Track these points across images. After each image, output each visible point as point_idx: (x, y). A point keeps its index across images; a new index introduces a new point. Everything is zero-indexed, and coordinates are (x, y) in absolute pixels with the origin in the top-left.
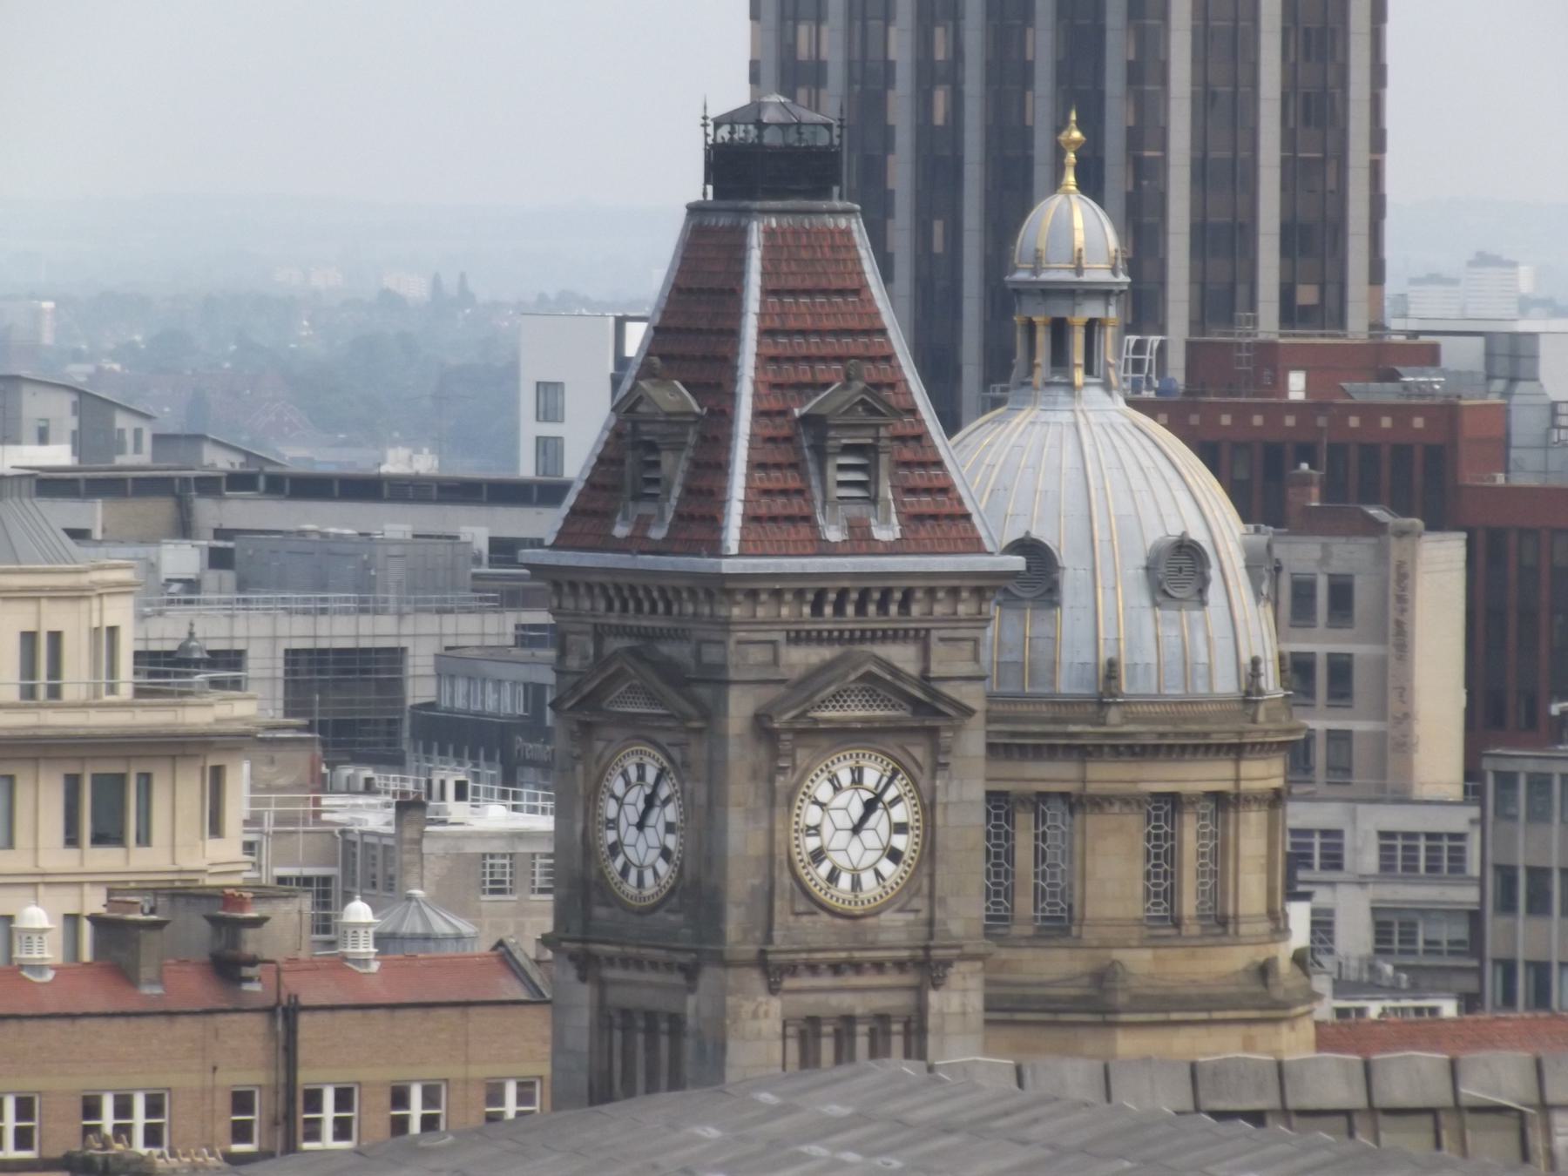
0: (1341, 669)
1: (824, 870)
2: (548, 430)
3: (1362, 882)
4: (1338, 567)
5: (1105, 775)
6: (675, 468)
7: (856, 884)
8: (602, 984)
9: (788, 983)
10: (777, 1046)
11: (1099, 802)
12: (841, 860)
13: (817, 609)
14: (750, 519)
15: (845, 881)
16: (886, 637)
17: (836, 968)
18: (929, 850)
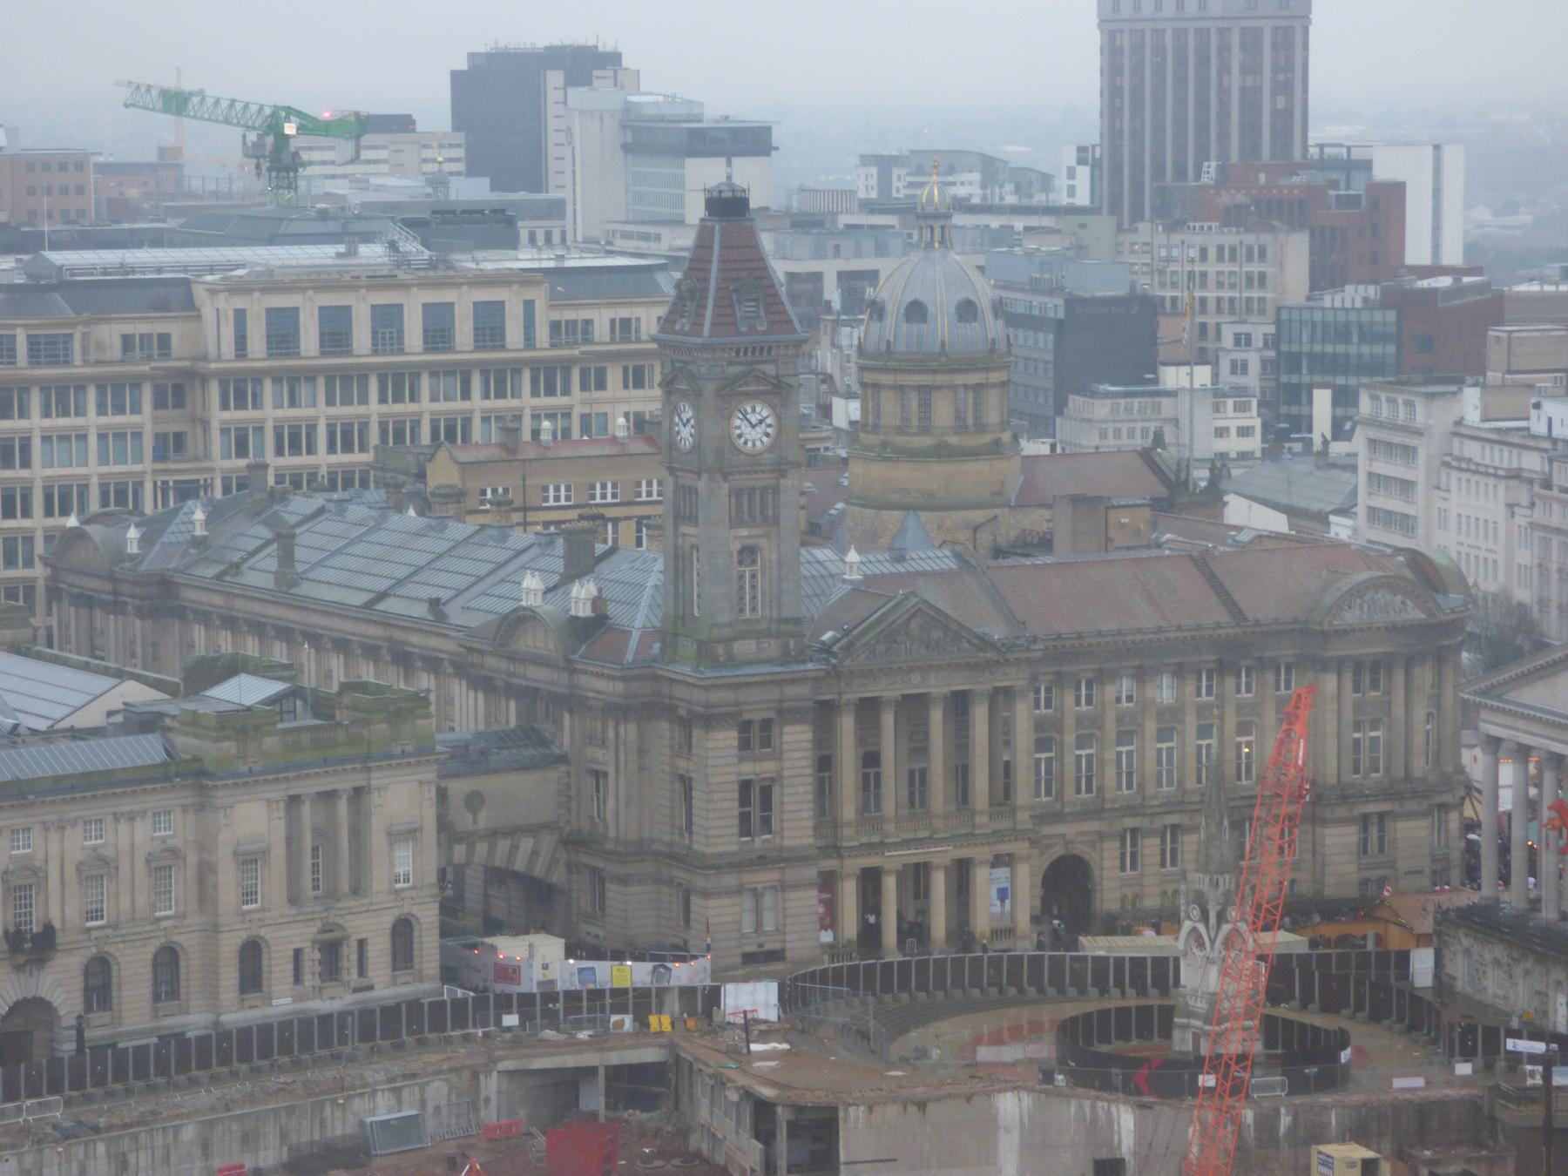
0: (1262, 277)
1: (742, 440)
2: (1071, 182)
3: (1258, 350)
4: (1262, 242)
5: (940, 379)
6: (690, 306)
7: (754, 444)
8: (676, 476)
9: (731, 478)
10: (727, 499)
11: (939, 388)
12: (748, 437)
13: (738, 353)
14: (713, 324)
15: (750, 444)
16: (766, 362)
17: (748, 473)
18: (779, 433)
